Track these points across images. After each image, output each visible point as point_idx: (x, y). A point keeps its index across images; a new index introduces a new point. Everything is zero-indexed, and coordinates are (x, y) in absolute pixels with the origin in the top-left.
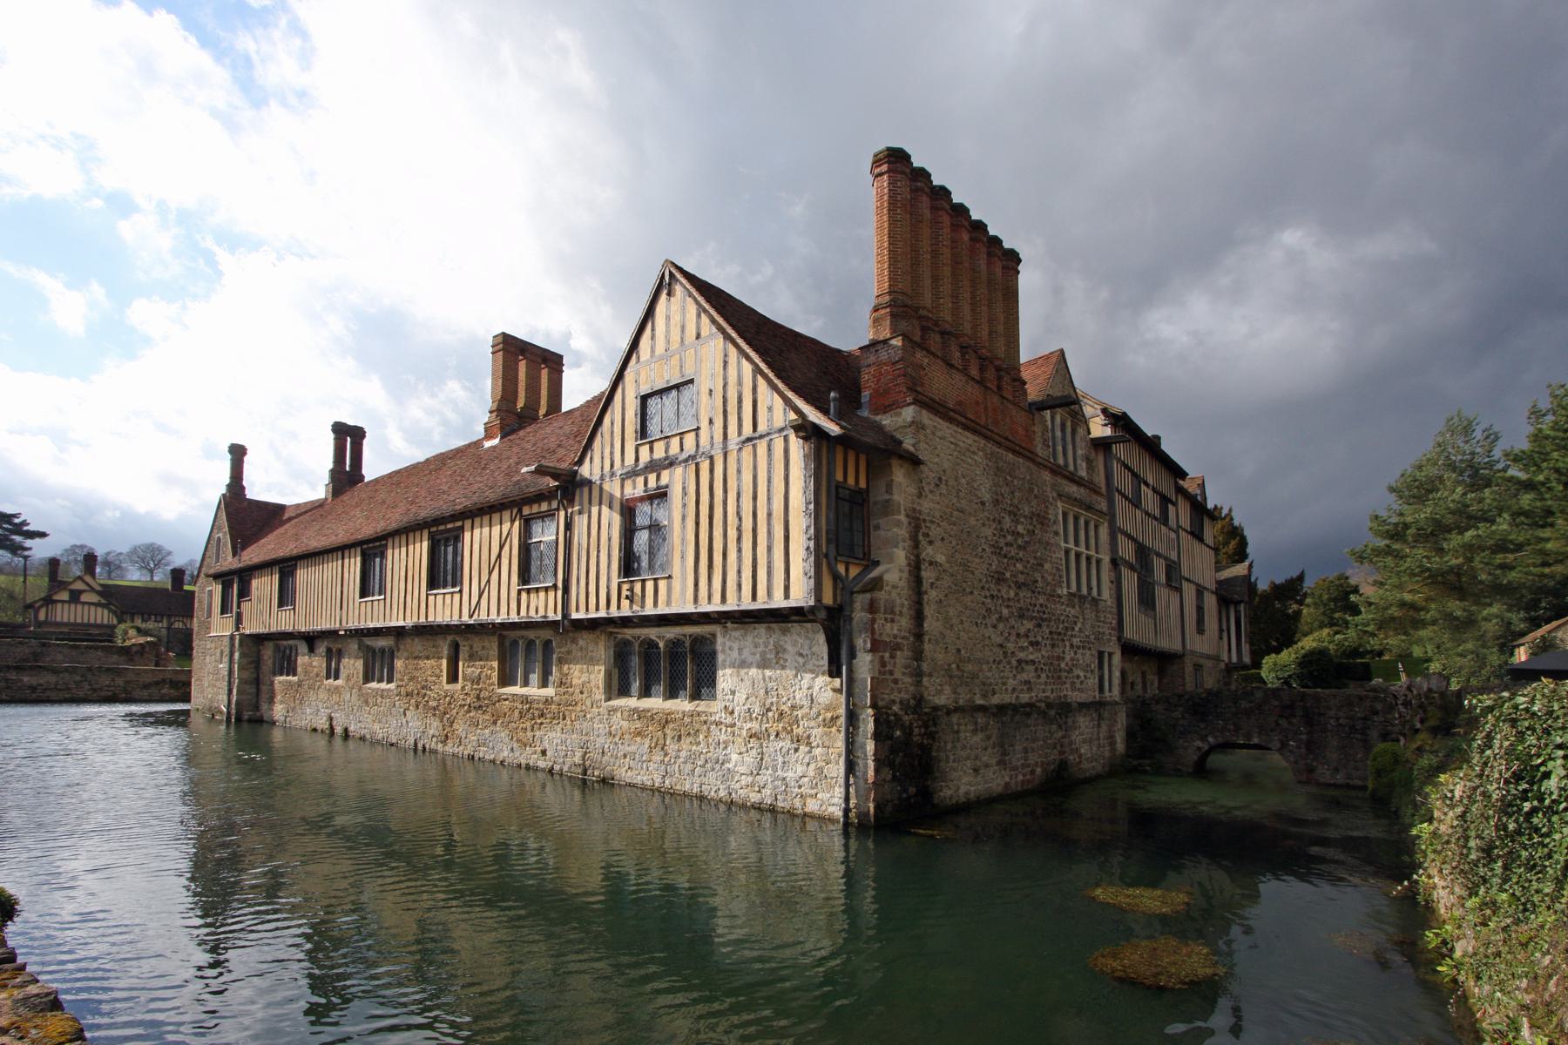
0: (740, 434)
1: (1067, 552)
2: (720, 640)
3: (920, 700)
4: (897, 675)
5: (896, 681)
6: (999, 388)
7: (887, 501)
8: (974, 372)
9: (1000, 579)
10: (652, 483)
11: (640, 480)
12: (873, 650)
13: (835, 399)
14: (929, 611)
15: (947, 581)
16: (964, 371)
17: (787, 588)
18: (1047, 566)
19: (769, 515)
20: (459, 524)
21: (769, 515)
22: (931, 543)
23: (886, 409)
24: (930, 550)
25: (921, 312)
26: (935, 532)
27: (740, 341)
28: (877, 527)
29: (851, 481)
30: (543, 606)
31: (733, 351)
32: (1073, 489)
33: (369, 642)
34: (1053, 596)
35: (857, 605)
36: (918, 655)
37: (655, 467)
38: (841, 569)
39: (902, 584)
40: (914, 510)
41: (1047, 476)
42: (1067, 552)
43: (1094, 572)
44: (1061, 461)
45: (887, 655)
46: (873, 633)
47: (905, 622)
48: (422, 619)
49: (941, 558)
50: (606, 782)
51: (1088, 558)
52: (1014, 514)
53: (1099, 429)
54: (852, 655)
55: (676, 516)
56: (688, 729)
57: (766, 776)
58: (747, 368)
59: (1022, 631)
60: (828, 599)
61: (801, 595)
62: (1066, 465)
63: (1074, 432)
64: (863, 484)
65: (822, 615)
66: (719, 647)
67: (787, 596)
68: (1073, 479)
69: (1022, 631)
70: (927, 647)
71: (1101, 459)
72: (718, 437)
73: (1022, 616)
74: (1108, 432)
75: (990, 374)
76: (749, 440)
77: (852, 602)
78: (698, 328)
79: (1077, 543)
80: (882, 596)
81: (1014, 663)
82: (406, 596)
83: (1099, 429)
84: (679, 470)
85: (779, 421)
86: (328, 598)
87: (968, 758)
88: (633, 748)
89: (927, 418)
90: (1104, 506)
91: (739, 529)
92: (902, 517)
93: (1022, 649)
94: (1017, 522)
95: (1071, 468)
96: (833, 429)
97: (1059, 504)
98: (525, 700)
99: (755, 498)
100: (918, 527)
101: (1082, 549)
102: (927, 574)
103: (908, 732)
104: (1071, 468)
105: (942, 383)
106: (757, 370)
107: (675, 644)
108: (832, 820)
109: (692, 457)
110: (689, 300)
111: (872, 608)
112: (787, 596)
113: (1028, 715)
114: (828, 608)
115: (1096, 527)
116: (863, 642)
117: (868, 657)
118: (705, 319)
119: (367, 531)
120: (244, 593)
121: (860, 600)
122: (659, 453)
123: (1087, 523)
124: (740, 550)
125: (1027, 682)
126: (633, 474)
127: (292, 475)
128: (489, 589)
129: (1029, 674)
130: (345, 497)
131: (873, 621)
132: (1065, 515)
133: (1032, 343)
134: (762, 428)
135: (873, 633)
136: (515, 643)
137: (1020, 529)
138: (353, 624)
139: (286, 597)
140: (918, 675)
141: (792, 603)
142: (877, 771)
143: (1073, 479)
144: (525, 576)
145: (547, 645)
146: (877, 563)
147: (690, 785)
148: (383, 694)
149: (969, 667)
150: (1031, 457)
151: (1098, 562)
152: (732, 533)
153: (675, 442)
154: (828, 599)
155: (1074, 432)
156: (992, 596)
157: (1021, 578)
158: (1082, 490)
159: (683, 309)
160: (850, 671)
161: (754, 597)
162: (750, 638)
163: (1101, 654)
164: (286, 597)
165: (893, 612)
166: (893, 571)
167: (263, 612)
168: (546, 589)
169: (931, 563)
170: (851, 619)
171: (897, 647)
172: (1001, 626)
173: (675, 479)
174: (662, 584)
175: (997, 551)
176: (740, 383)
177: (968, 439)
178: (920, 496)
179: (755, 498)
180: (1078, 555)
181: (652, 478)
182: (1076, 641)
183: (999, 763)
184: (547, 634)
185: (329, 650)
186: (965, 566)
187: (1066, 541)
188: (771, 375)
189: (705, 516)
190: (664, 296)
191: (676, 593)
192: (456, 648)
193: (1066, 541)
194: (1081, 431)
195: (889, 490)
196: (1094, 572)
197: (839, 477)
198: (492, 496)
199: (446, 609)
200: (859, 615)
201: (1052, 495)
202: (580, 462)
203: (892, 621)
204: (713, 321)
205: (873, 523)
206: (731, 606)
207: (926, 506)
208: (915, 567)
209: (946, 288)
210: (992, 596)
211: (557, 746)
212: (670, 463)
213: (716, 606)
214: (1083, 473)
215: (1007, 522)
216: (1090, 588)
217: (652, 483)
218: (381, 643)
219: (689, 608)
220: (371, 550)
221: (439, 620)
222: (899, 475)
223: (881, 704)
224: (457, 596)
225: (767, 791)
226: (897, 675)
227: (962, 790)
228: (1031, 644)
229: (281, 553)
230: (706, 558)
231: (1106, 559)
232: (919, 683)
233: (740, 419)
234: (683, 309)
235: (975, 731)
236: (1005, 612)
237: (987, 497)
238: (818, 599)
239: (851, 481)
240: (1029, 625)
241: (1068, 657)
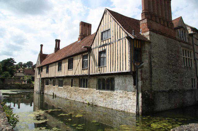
0: (118, 39)
1: (184, 58)
2: (115, 78)
3: (151, 90)
4: (147, 85)
5: (146, 86)
6: (168, 26)
7: (144, 50)
8: (162, 23)
9: (169, 64)
10: (103, 49)
11: (101, 48)
12: (141, 80)
13: (134, 31)
14: (153, 72)
15: (157, 65)
16: (160, 23)
17: (126, 68)
18: (179, 61)
19: (123, 54)
20: (73, 57)
21: (123, 54)
22: (153, 58)
23: (145, 32)
24: (153, 59)
25: (151, 13)
26: (154, 56)
27: (117, 22)
28: (143, 55)
29: (137, 47)
30: (85, 72)
31: (116, 24)
32: (185, 45)
33: (59, 79)
34: (181, 67)
35: (139, 71)
36: (151, 81)
37: (104, 45)
38: (136, 64)
39: (148, 66)
40: (150, 51)
41: (178, 42)
42: (184, 58)
43: (190, 61)
44: (182, 39)
45: (144, 81)
46: (141, 76)
47: (148, 74)
48: (67, 75)
49: (156, 61)
50: (96, 106)
51: (189, 59)
52: (172, 51)
53: (190, 32)
54: (138, 81)
55: (108, 56)
56: (110, 96)
57: (123, 105)
58: (119, 26)
59: (174, 75)
60: (133, 70)
61: (128, 69)
62: (183, 40)
63: (185, 33)
64: (140, 47)
65: (132, 73)
66: (115, 80)
67: (126, 70)
68: (185, 42)
69: (174, 75)
70: (153, 79)
71: (191, 38)
72: (114, 40)
73: (174, 72)
74: (192, 32)
75: (166, 23)
76: (119, 40)
77: (138, 70)
78: (111, 20)
79: (186, 56)
80: (143, 69)
81: (172, 82)
82: (65, 72)
83: (190, 32)
84: (108, 46)
85: (124, 36)
86: (53, 72)
88: (100, 100)
89: (152, 33)
90: (192, 48)
91: (118, 57)
92: (147, 53)
93: (174, 79)
94: (172, 52)
95: (185, 40)
96: (133, 38)
97: (182, 48)
98: (83, 90)
99: (120, 51)
100: (151, 55)
101: (187, 57)
102: (153, 64)
103: (149, 96)
104: (185, 40)
105: (155, 26)
106: (120, 27)
107: (108, 79)
108: (134, 114)
109: (110, 44)
110: (109, 15)
111: (141, 71)
112: (126, 70)
113: (175, 92)
114: (133, 72)
115: (190, 52)
116: (139, 78)
117: (141, 81)
118: (112, 18)
119: (59, 59)
120: (42, 71)
121: (139, 70)
122: (104, 43)
123: (188, 52)
124: (118, 61)
125: (175, 86)
126: (100, 47)
127: (49, 50)
128: (77, 70)
129: (175, 84)
130: (57, 53)
131: (142, 74)
132: (183, 50)
133: (175, 16)
134: (121, 38)
135: (141, 76)
136: (82, 79)
137: (173, 54)
138: (57, 76)
139: (47, 72)
140: (151, 85)
141: (126, 71)
142: (142, 104)
143: (185, 42)
144: (83, 67)
145: (87, 79)
146: (143, 63)
147: (110, 107)
148: (61, 89)
149: (162, 83)
150: (175, 39)
151: (191, 59)
152: (116, 58)
153: (107, 41)
154: (133, 70)
155: (185, 33)
156: (167, 68)
157: (173, 64)
158: (187, 45)
159: (108, 16)
160: (137, 84)
161: (115, 71)
162: (120, 78)
163: (192, 79)
164: (47, 72)
165: (146, 72)
166: (146, 63)
167: (44, 74)
168: (86, 69)
169: (154, 62)
170: (138, 74)
171: (147, 79)
172: (169, 74)
173: (107, 48)
174: (105, 68)
175: (168, 59)
176: (117, 29)
177: (161, 36)
178: (151, 49)
179: (120, 51)
180: (186, 58)
181: (103, 47)
182: (186, 77)
183: (169, 103)
184: (86, 78)
185: (53, 81)
186: (161, 62)
187: (183, 55)
188: (122, 28)
189: (112, 55)
190: (105, 14)
191: (107, 70)
192: (72, 80)
193: (183, 55)
194: (186, 33)
195: (145, 48)
196: (190, 61)
197: (135, 46)
198: (78, 52)
199: (71, 73)
200: (139, 73)
201: (180, 46)
202: (92, 45)
203: (145, 74)
204: (113, 18)
205: (142, 55)
206: (116, 72)
207: (152, 51)
208: (150, 63)
209: (156, 8)
210: (167, 68)
211: (88, 99)
212: (106, 45)
213: (114, 72)
214: (187, 41)
215: (170, 53)
216: (189, 65)
217: (103, 49)
218: (61, 79)
219: (109, 72)
220: (60, 63)
221: (69, 75)
222: (147, 45)
223: (143, 91)
224: (72, 71)
225: (123, 108)
226: (147, 85)
228: (176, 77)
229: (47, 63)
230: (112, 62)
231: (193, 58)
232: (151, 86)
233: (118, 36)
234: (108, 16)
235: (163, 96)
236: (170, 71)
237: (165, 48)
238: (131, 70)
239: (137, 47)
240: (175, 74)
241: (184, 80)
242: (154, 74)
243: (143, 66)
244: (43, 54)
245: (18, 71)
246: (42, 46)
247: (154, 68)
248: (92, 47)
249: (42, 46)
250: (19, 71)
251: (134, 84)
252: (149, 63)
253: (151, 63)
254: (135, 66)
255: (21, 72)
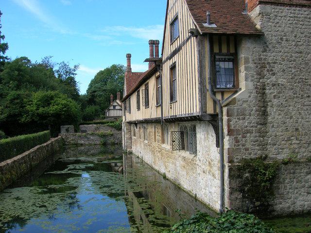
5: (247, 149)
22: (274, 74)
26: (277, 68)
36: (263, 134)
40: (260, 59)
47: (254, 119)
54: (223, 138)
87: (304, 187)
89: (269, 8)
116: (226, 131)
140: (263, 146)
165: (243, 114)
169: (274, 85)
207: (270, 56)
226: (248, 146)
227: (299, 203)
242: (274, 115)
243: (235, 98)
244: (133, 73)
245: (112, 108)
246: (129, 56)
247: (275, 101)
248: (163, 60)
249: (129, 56)
250: (114, 107)
251: (218, 146)
252: (256, 88)
253: (264, 89)
254: (215, 102)
255: (116, 108)
